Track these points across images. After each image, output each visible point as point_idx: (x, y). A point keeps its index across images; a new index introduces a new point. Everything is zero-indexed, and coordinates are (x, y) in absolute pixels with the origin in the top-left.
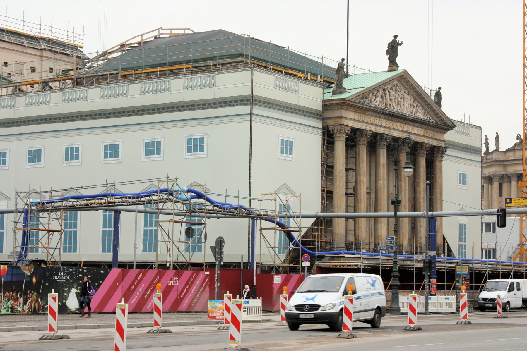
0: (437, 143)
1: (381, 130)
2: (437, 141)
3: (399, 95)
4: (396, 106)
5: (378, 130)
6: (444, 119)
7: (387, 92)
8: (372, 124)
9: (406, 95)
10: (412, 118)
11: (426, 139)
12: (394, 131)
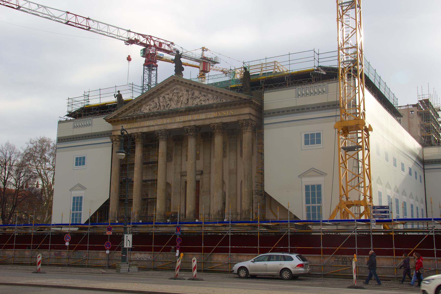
0: (236, 119)
1: (156, 128)
2: (237, 117)
3: (175, 96)
4: (175, 104)
5: (151, 129)
6: (236, 96)
7: (161, 99)
8: (143, 127)
9: (185, 93)
10: (185, 109)
11: (217, 119)
12: (171, 125)
